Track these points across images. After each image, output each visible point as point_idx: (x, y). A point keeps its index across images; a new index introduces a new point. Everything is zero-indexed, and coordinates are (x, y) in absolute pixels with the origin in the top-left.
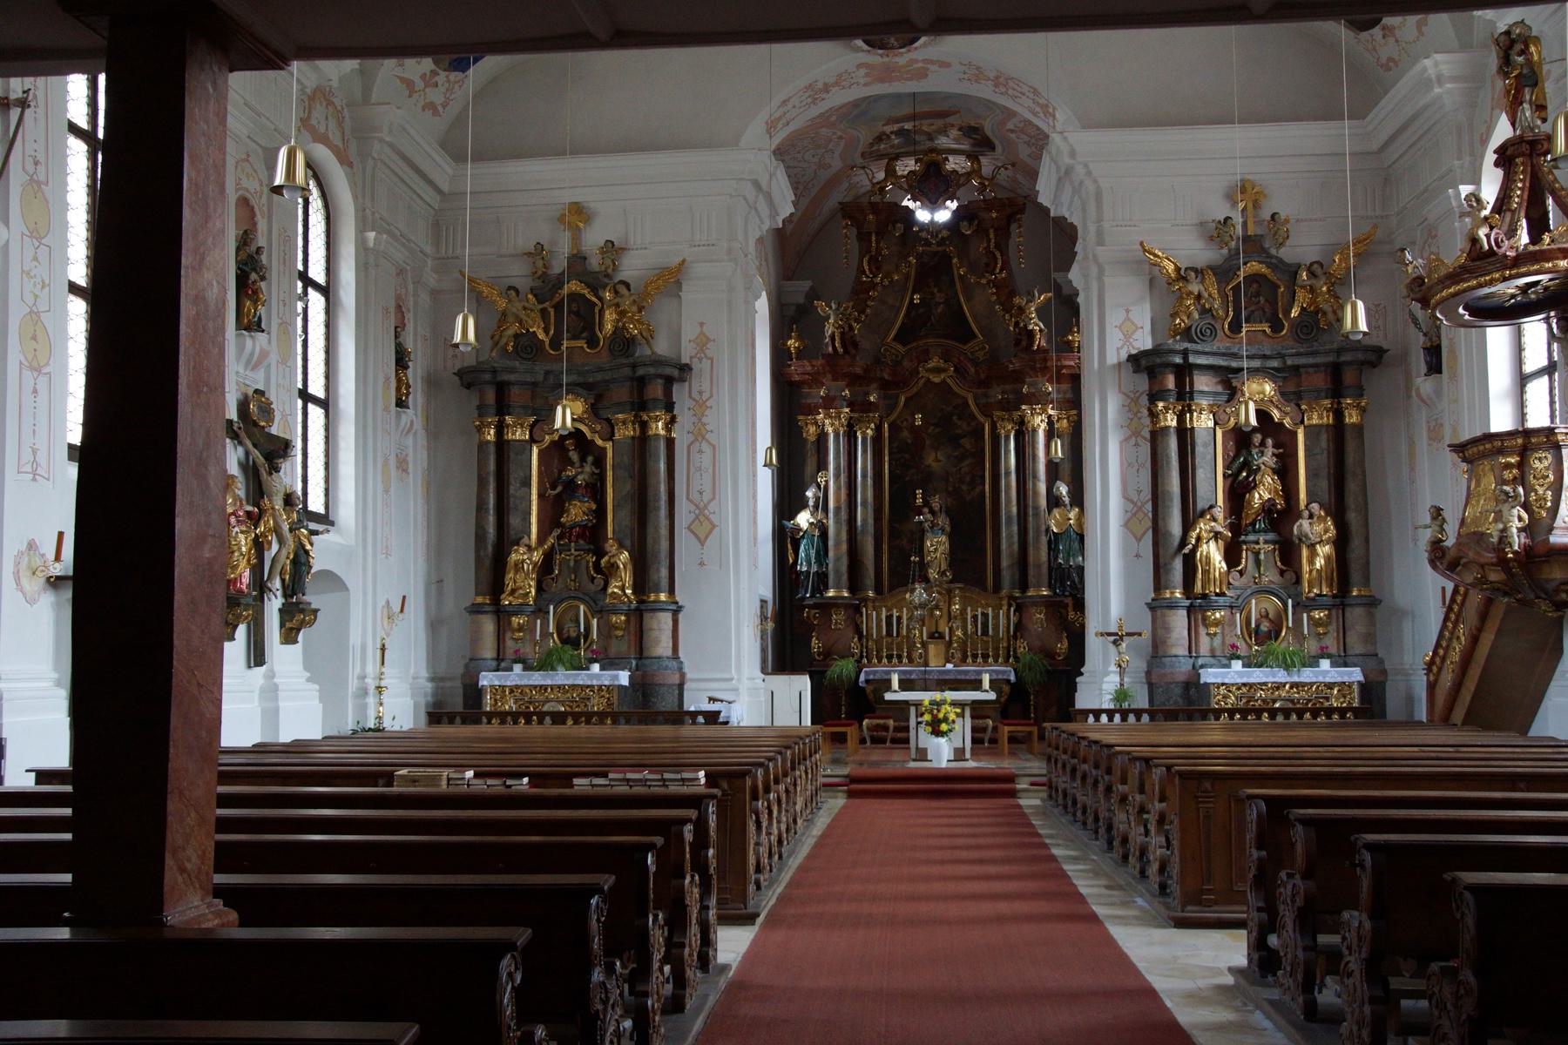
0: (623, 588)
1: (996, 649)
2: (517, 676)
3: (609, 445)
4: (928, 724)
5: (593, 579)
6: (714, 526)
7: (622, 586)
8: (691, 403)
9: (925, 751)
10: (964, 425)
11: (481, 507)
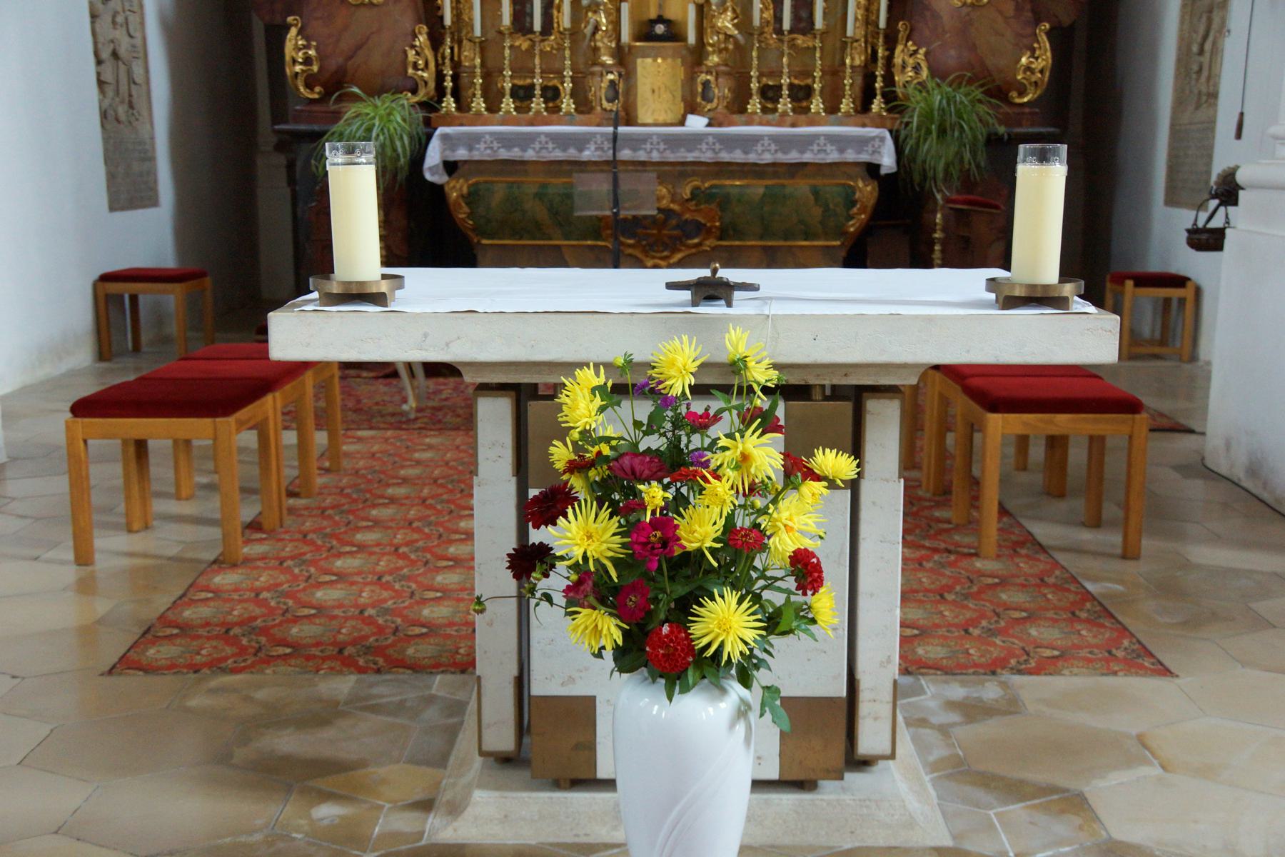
1: (834, 73)
4: (590, 587)
9: (579, 714)
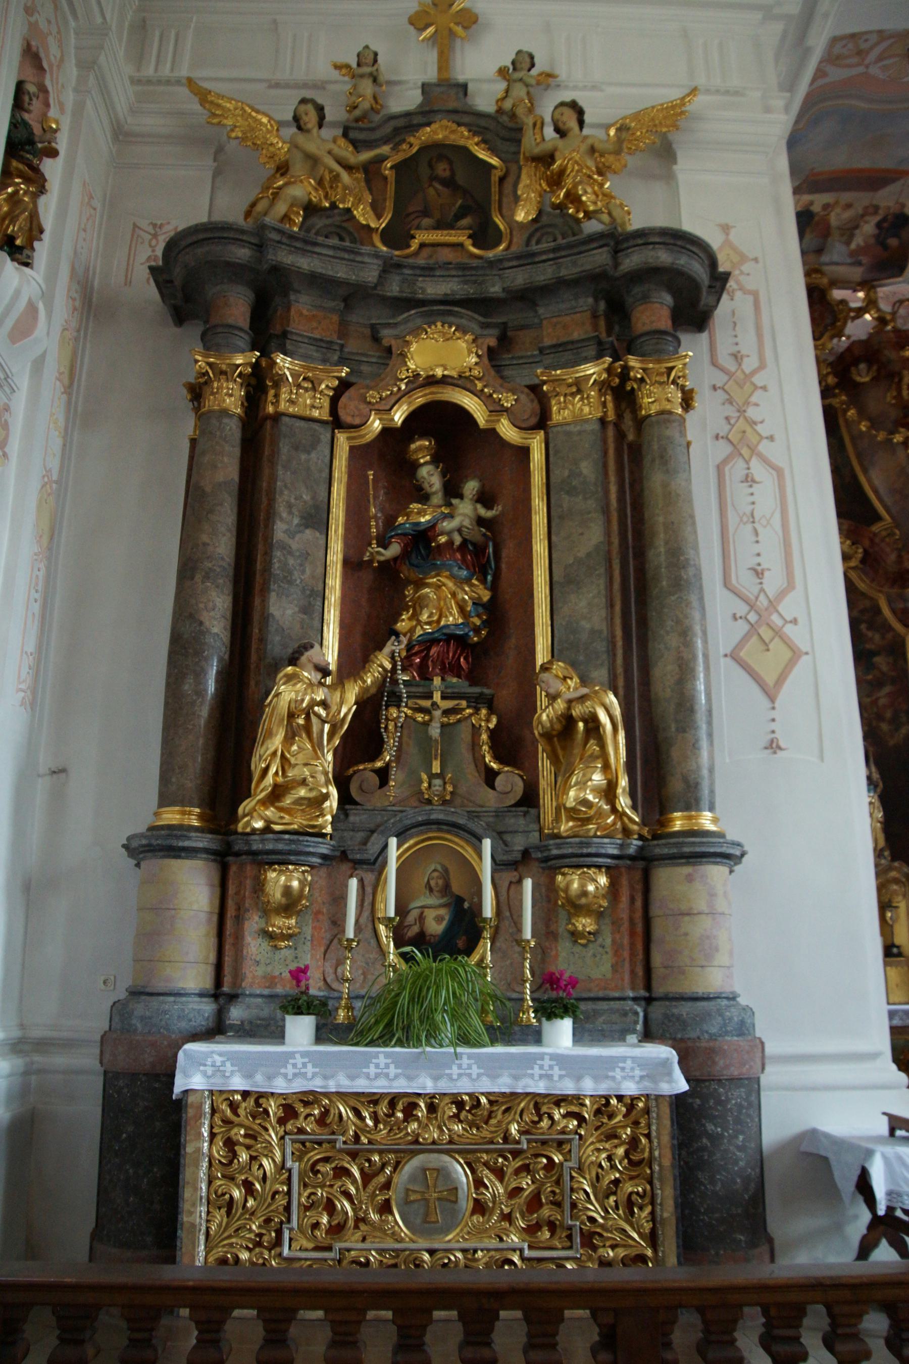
0: (609, 792)
2: (298, 1060)
3: (537, 446)
5: (490, 777)
6: (796, 654)
7: (592, 789)
8: (720, 379)
10: (877, 637)
11: (188, 569)
